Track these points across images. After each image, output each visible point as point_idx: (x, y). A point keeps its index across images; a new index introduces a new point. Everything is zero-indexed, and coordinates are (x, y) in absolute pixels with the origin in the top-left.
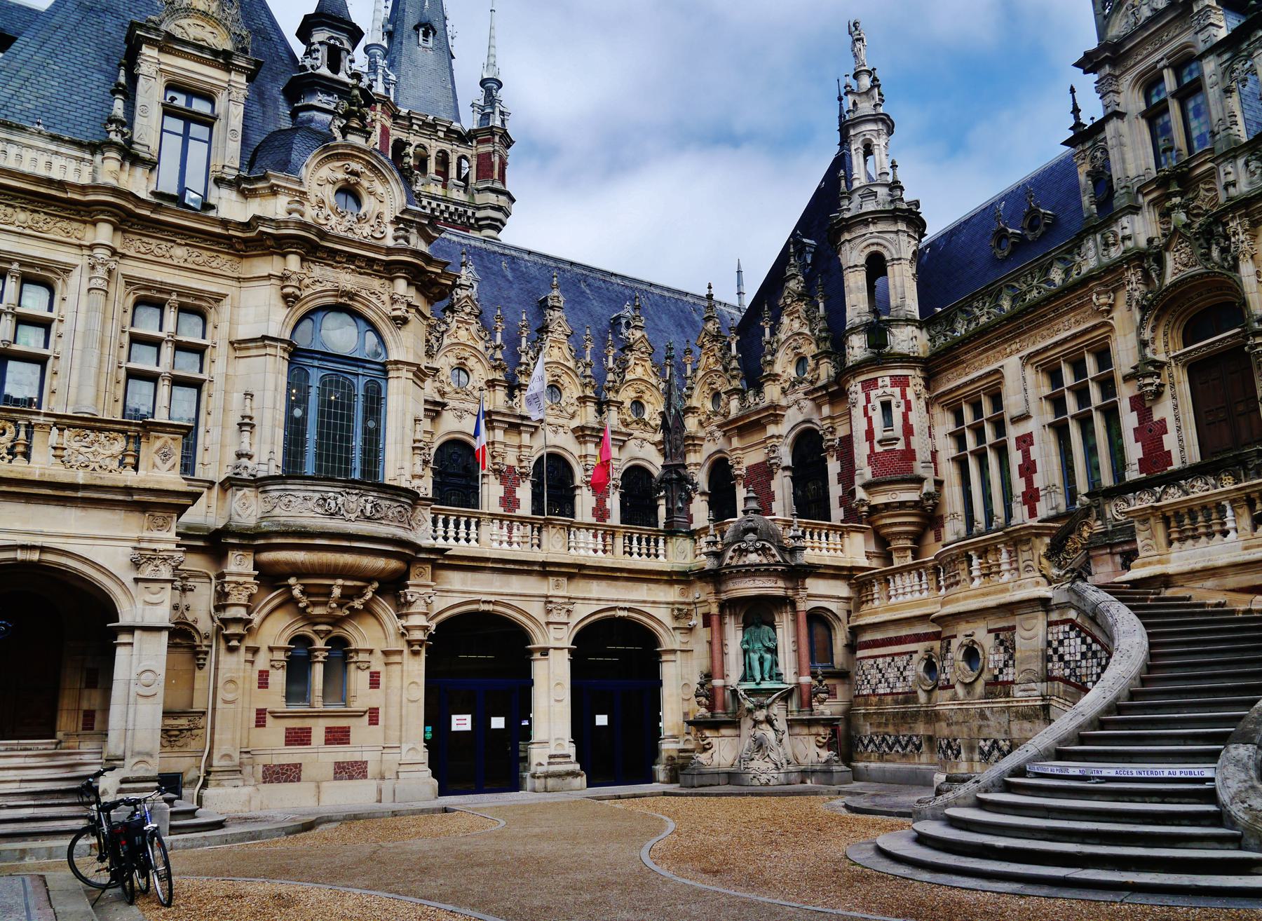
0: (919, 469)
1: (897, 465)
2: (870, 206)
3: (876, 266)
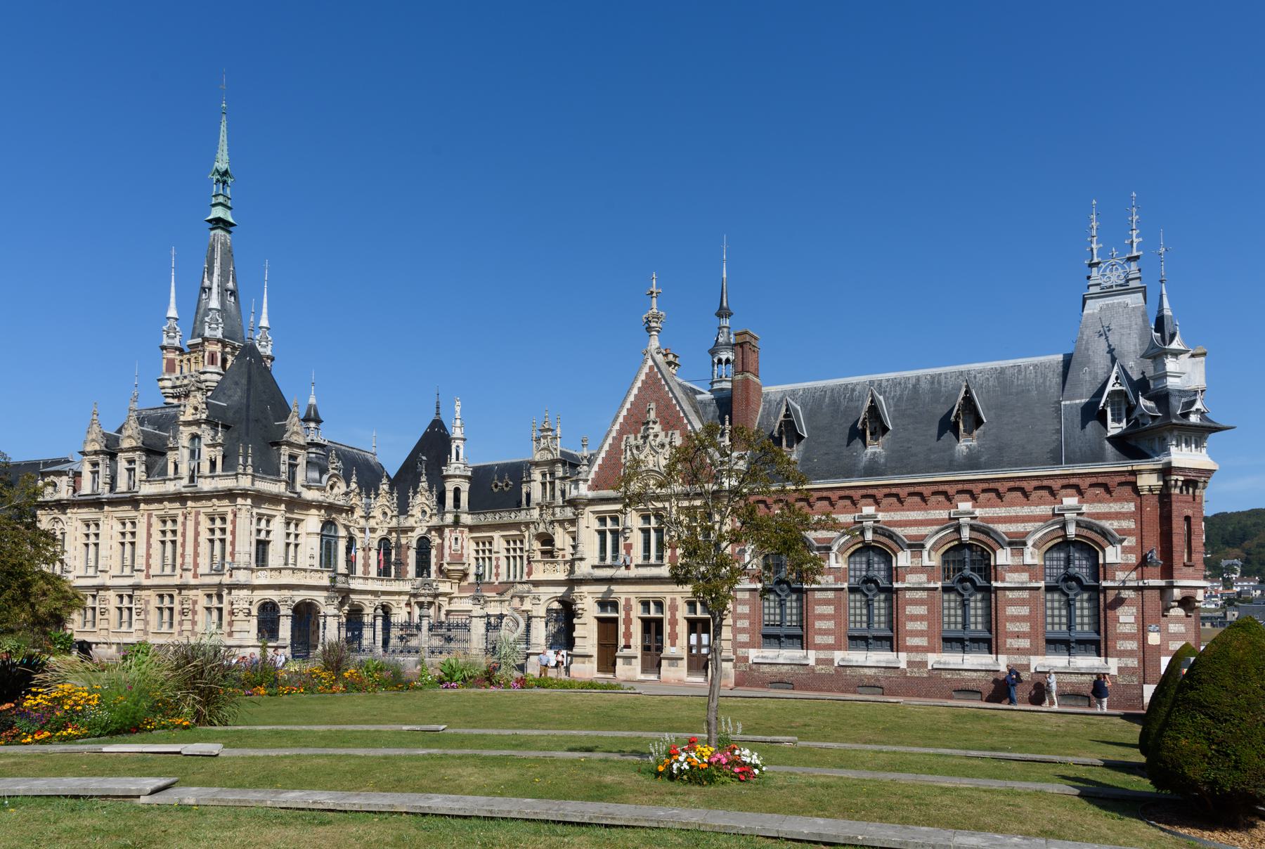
0: (464, 560)
1: (458, 558)
2: (458, 472)
3: (457, 491)
